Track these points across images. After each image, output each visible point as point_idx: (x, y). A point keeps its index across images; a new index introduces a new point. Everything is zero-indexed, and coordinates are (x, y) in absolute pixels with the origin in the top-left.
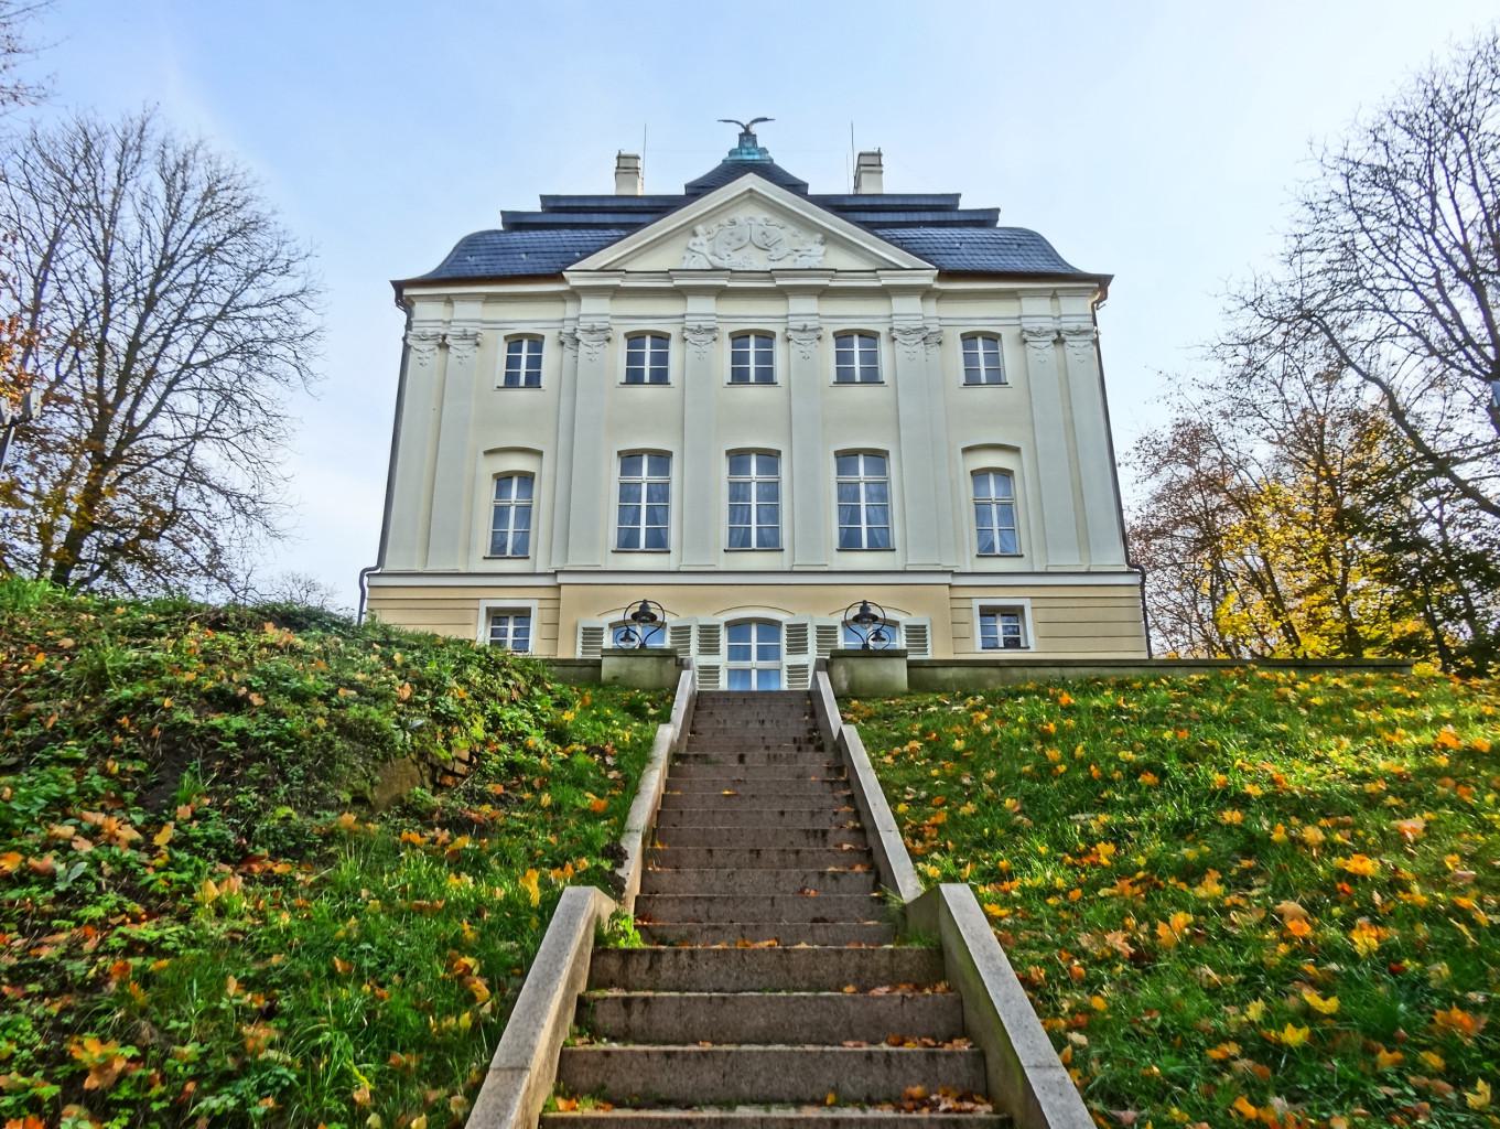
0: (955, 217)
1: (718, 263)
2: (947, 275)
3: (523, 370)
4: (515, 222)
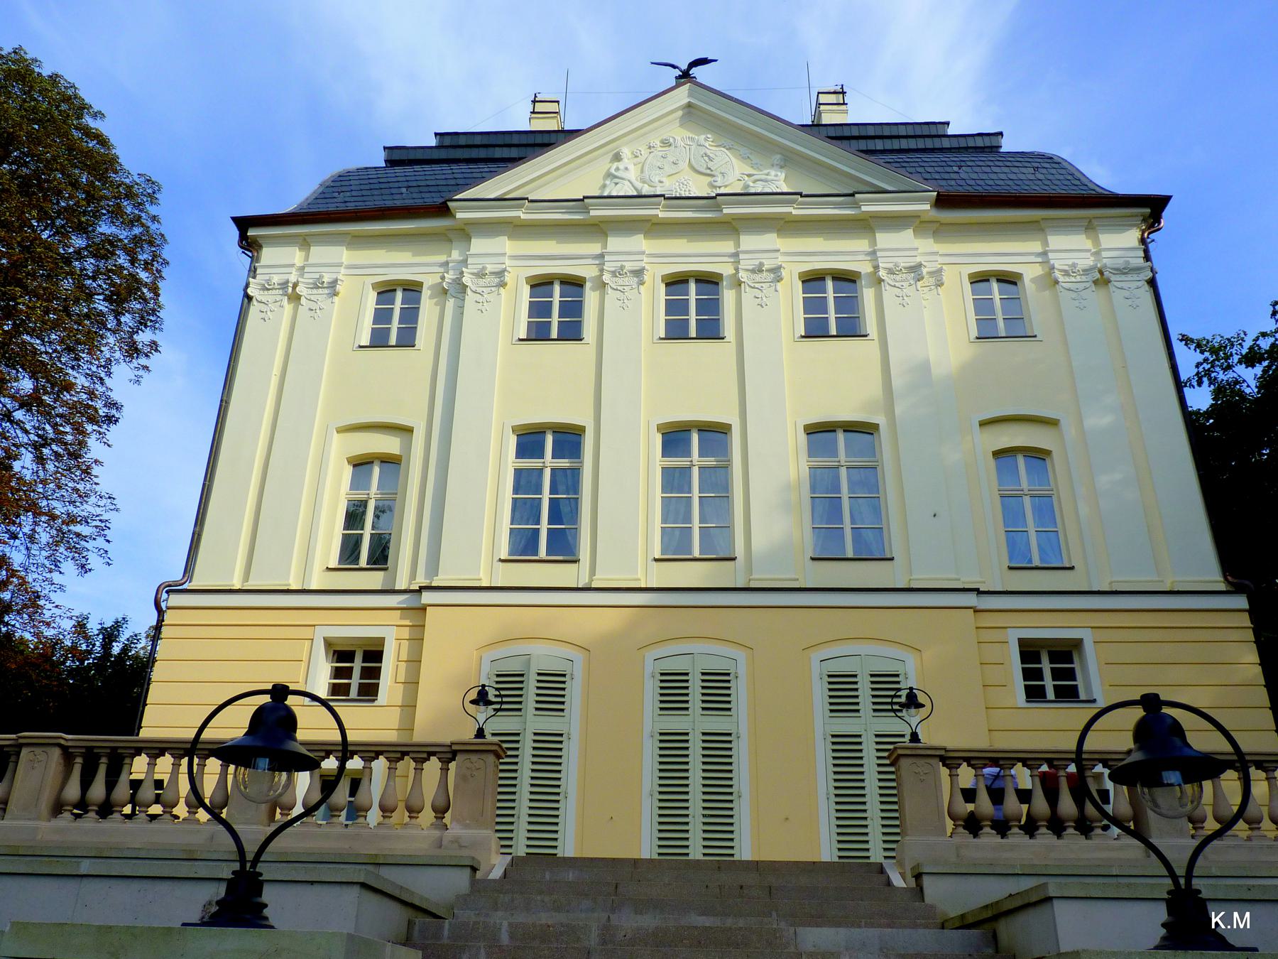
0: (946, 143)
1: (646, 190)
2: (944, 201)
3: (395, 325)
4: (399, 158)
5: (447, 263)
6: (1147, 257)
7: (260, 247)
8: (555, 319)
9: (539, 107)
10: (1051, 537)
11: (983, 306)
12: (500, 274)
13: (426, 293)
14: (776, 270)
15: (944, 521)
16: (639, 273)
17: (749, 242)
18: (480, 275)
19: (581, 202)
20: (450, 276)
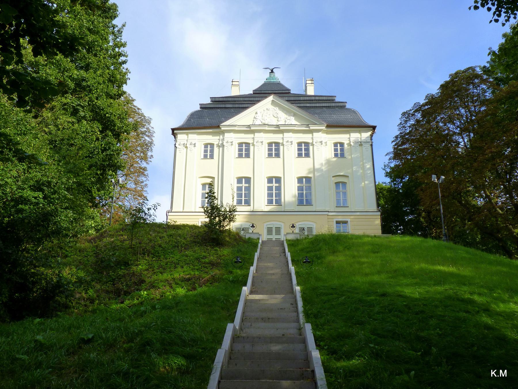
0: (333, 105)
1: (263, 122)
2: (328, 126)
3: (209, 153)
4: (204, 107)
5: (219, 139)
6: (371, 139)
7: (177, 135)
8: (244, 152)
9: (234, 83)
10: (345, 201)
11: (336, 150)
12: (232, 142)
13: (215, 146)
14: (291, 142)
15: (324, 199)
16: (262, 142)
17: (286, 135)
18: (227, 142)
19: (249, 126)
20: (221, 142)
